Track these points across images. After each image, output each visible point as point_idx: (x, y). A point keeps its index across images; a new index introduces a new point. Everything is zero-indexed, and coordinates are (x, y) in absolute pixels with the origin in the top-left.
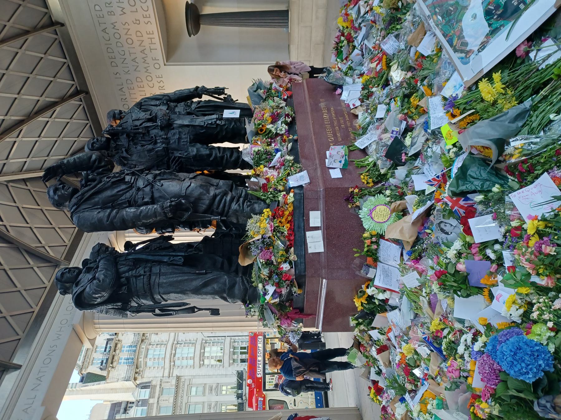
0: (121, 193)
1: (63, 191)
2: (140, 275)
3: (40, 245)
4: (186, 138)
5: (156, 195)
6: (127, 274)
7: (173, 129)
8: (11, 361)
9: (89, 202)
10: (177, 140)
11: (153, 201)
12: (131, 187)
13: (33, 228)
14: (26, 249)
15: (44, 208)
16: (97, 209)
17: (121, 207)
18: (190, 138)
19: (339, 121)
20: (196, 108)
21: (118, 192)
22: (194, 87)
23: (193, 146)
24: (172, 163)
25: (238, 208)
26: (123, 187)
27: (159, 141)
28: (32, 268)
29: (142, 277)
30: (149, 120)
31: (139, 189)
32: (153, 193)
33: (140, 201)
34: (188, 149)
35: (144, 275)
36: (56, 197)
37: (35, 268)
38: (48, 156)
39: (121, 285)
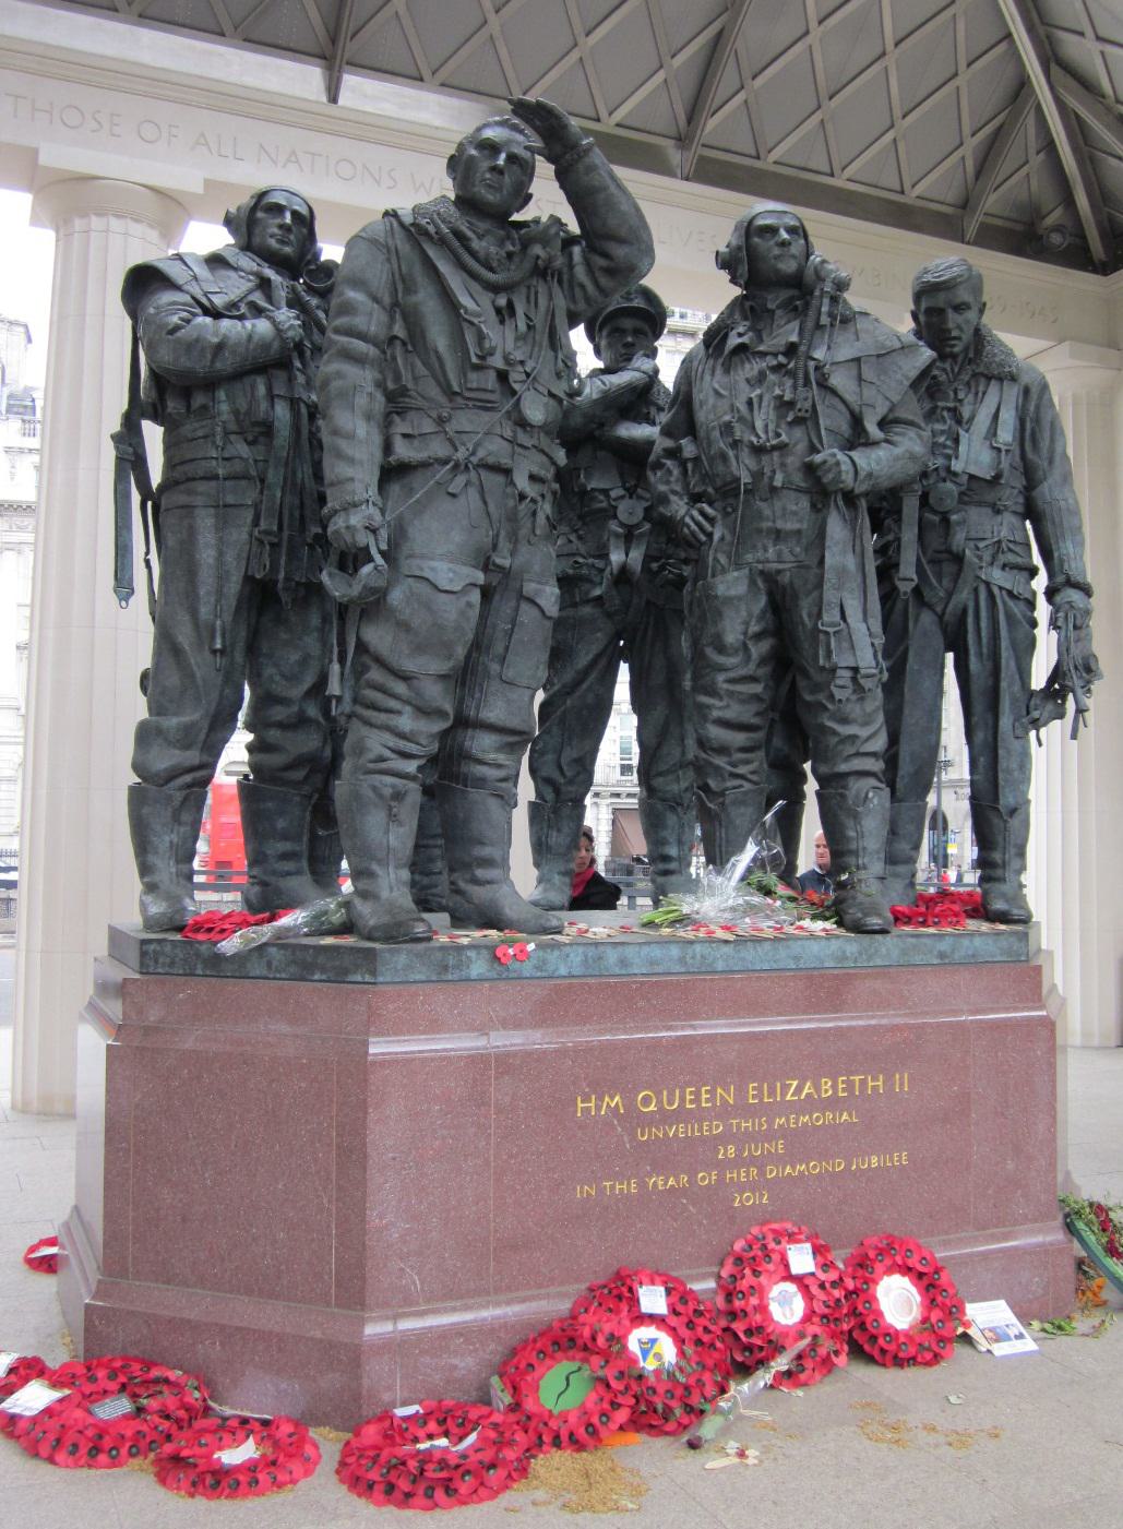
3: (747, 74)
4: (769, 555)
8: (346, 67)
10: (766, 525)
12: (451, 394)
13: (808, 40)
14: (725, 33)
15: (890, 61)
18: (779, 572)
19: (769, 1136)
20: (988, 584)
22: (1089, 579)
23: (752, 582)
24: (703, 513)
25: (371, 756)
27: (765, 459)
28: (661, 67)
30: (857, 421)
33: (401, 427)
34: (738, 566)
37: (661, 76)
38: (1099, 38)
39: (186, 393)
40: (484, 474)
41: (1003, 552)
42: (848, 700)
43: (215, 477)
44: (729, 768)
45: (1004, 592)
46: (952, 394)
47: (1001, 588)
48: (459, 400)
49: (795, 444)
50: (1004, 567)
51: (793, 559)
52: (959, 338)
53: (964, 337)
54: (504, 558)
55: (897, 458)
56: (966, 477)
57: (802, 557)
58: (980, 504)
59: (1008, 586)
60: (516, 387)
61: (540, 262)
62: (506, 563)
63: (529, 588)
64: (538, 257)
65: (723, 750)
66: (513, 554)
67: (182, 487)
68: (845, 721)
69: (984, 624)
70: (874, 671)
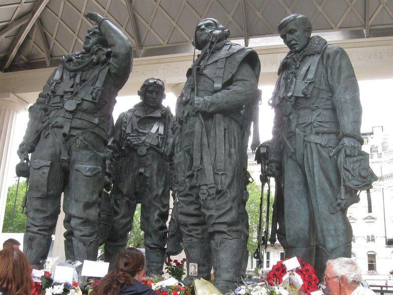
40: (56, 129)
41: (315, 127)
42: (206, 199)
44: (186, 232)
45: (319, 146)
46: (294, 66)
47: (316, 144)
50: (317, 133)
52: (297, 44)
53: (298, 43)
54: (65, 156)
55: (228, 95)
56: (293, 98)
58: (305, 108)
59: (319, 142)
60: (65, 99)
61: (94, 60)
62: (66, 158)
63: (77, 166)
64: (94, 59)
65: (185, 225)
66: (69, 154)
68: (208, 209)
69: (310, 161)
70: (214, 185)
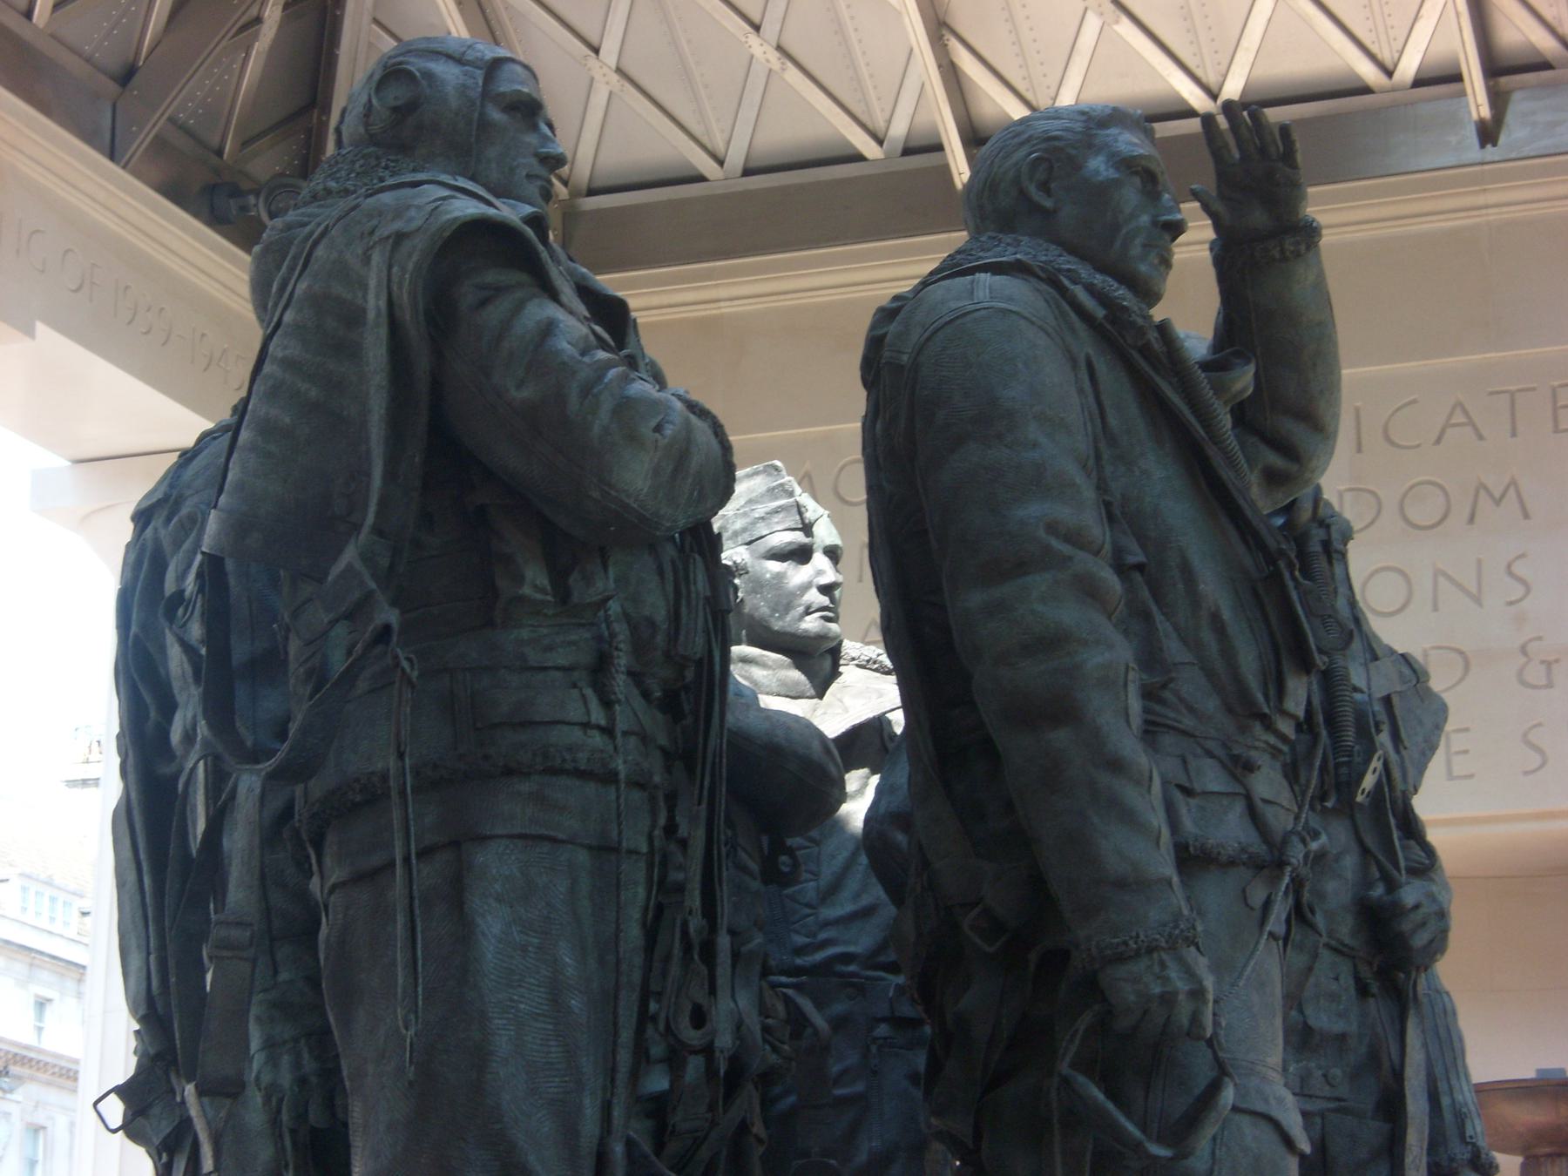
0: (1207, 636)
1: (1145, 219)
2: (607, 704)
5: (1217, 893)
6: (614, 607)
7: (1363, 991)
9: (1133, 409)
11: (1193, 860)
12: (1245, 710)
16: (1098, 457)
17: (1138, 621)
21: (1216, 618)
26: (1249, 661)
29: (598, 716)
31: (1239, 767)
32: (1232, 863)
35: (608, 731)
36: (1098, 166)
43: (610, 778)
48: (1258, 729)
49: (1337, 858)
51: (1327, 1091)
57: (1343, 1090)
67: (525, 787)
